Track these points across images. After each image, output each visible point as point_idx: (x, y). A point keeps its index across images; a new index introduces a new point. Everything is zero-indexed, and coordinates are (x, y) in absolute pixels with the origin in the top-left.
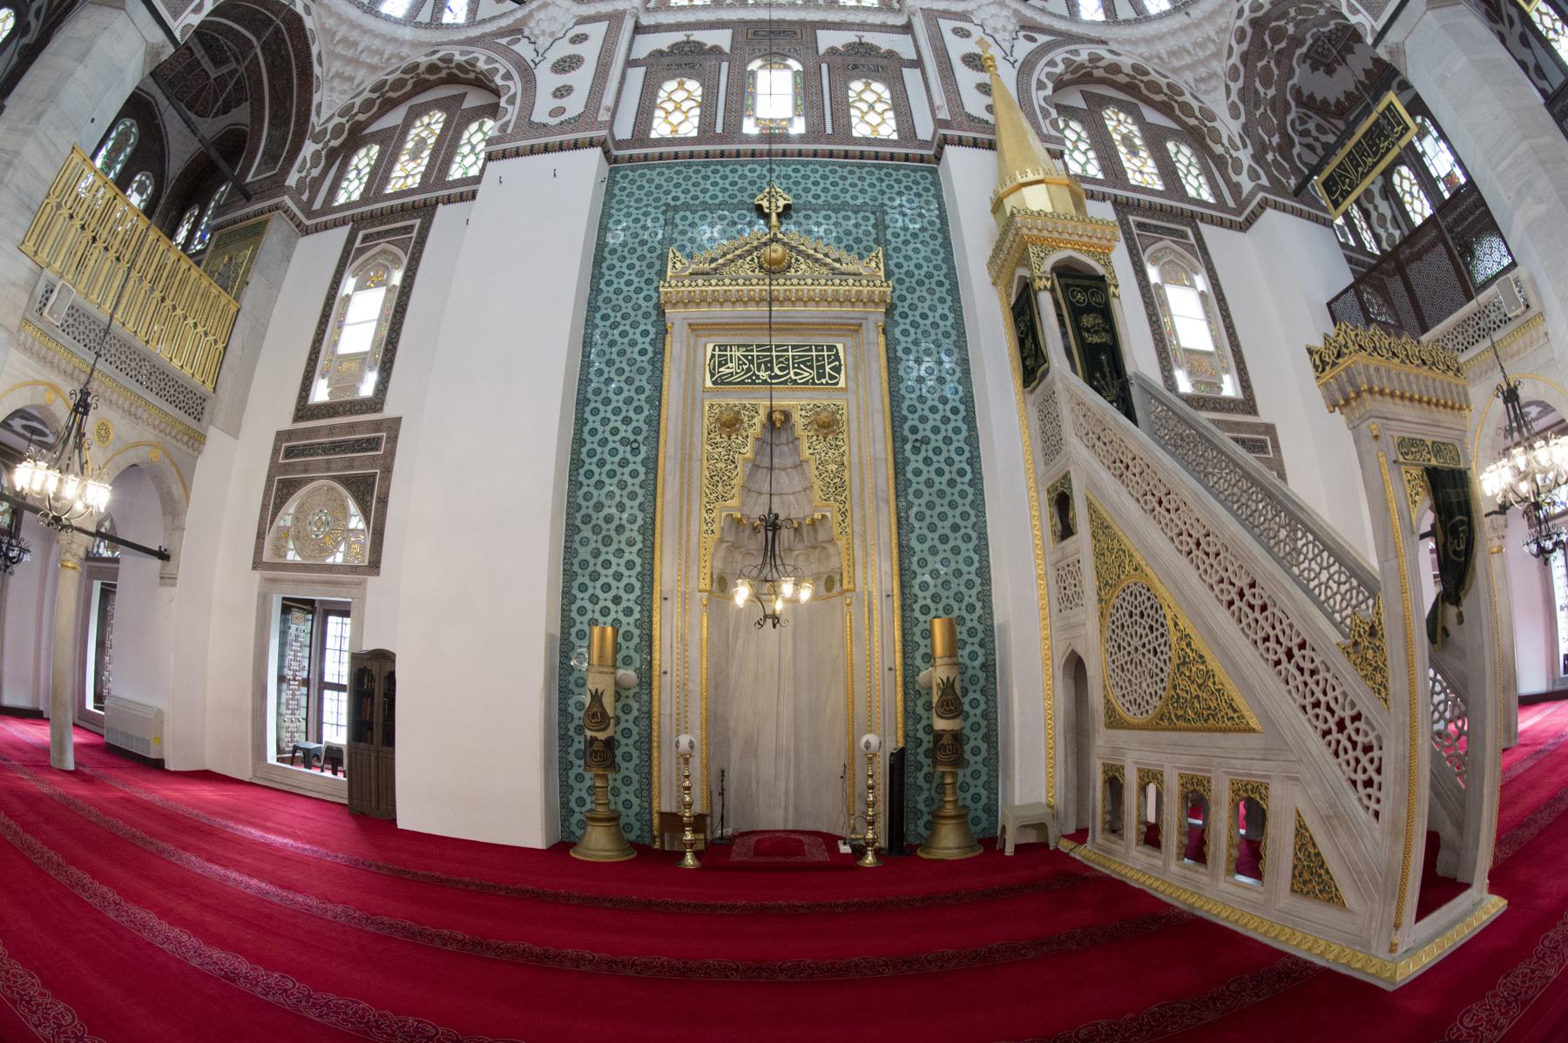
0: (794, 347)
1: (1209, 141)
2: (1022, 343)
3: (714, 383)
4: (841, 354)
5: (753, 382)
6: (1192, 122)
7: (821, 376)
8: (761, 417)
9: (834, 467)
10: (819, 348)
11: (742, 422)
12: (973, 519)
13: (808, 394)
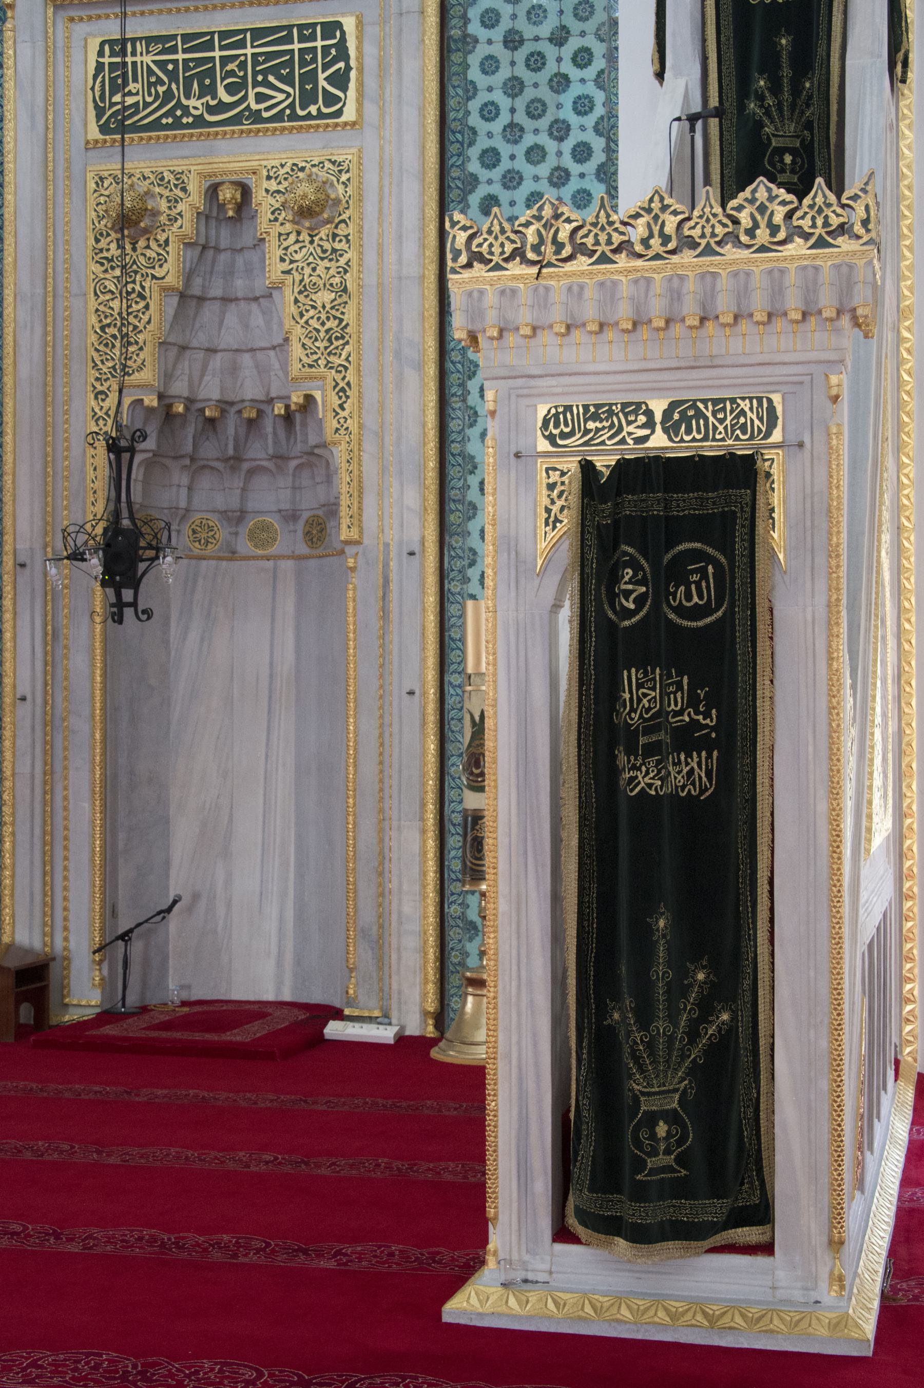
0: (258, 33)
3: (104, 129)
4: (351, 45)
5: (177, 124)
7: (308, 98)
8: (195, 197)
9: (325, 297)
10: (306, 31)
11: (155, 213)
13: (283, 141)
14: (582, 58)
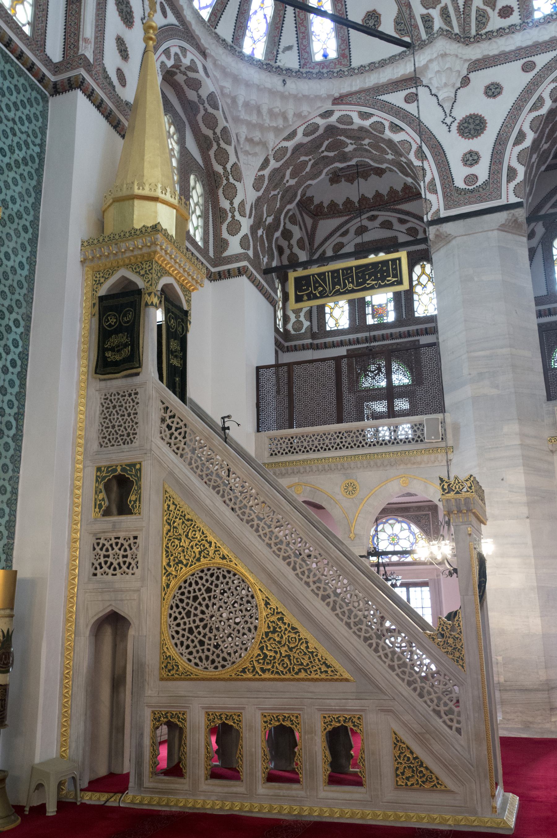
1: (220, 191)
2: (104, 334)
6: (219, 169)
12: (10, 473)
14: (17, 323)
